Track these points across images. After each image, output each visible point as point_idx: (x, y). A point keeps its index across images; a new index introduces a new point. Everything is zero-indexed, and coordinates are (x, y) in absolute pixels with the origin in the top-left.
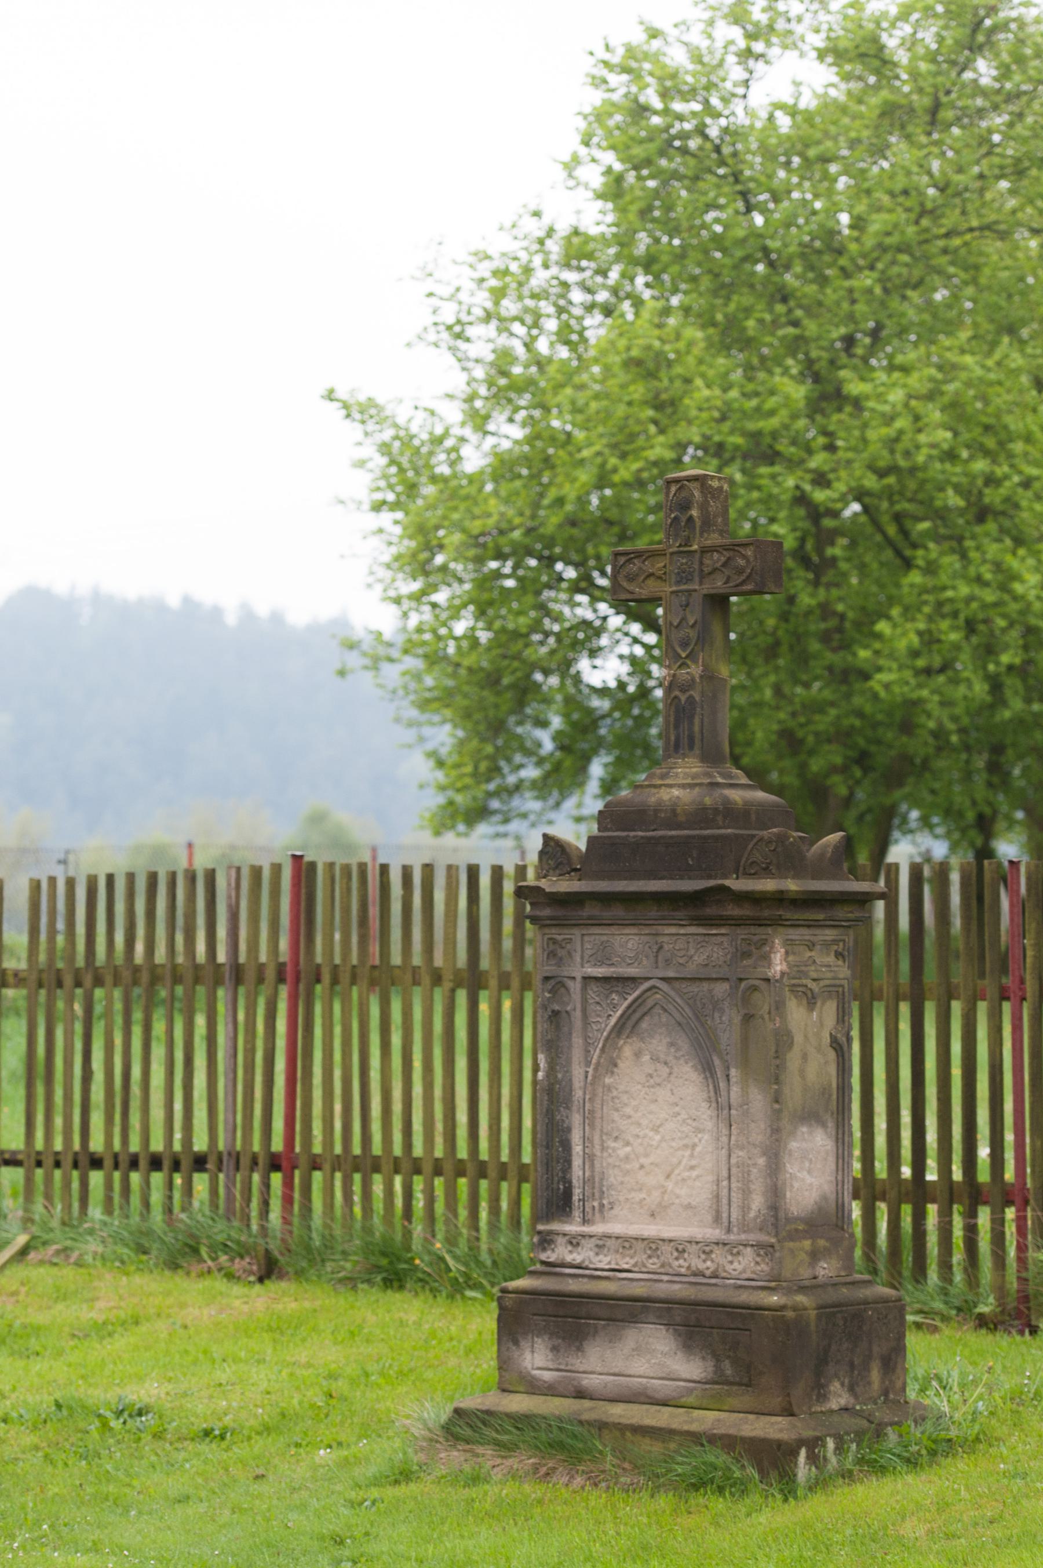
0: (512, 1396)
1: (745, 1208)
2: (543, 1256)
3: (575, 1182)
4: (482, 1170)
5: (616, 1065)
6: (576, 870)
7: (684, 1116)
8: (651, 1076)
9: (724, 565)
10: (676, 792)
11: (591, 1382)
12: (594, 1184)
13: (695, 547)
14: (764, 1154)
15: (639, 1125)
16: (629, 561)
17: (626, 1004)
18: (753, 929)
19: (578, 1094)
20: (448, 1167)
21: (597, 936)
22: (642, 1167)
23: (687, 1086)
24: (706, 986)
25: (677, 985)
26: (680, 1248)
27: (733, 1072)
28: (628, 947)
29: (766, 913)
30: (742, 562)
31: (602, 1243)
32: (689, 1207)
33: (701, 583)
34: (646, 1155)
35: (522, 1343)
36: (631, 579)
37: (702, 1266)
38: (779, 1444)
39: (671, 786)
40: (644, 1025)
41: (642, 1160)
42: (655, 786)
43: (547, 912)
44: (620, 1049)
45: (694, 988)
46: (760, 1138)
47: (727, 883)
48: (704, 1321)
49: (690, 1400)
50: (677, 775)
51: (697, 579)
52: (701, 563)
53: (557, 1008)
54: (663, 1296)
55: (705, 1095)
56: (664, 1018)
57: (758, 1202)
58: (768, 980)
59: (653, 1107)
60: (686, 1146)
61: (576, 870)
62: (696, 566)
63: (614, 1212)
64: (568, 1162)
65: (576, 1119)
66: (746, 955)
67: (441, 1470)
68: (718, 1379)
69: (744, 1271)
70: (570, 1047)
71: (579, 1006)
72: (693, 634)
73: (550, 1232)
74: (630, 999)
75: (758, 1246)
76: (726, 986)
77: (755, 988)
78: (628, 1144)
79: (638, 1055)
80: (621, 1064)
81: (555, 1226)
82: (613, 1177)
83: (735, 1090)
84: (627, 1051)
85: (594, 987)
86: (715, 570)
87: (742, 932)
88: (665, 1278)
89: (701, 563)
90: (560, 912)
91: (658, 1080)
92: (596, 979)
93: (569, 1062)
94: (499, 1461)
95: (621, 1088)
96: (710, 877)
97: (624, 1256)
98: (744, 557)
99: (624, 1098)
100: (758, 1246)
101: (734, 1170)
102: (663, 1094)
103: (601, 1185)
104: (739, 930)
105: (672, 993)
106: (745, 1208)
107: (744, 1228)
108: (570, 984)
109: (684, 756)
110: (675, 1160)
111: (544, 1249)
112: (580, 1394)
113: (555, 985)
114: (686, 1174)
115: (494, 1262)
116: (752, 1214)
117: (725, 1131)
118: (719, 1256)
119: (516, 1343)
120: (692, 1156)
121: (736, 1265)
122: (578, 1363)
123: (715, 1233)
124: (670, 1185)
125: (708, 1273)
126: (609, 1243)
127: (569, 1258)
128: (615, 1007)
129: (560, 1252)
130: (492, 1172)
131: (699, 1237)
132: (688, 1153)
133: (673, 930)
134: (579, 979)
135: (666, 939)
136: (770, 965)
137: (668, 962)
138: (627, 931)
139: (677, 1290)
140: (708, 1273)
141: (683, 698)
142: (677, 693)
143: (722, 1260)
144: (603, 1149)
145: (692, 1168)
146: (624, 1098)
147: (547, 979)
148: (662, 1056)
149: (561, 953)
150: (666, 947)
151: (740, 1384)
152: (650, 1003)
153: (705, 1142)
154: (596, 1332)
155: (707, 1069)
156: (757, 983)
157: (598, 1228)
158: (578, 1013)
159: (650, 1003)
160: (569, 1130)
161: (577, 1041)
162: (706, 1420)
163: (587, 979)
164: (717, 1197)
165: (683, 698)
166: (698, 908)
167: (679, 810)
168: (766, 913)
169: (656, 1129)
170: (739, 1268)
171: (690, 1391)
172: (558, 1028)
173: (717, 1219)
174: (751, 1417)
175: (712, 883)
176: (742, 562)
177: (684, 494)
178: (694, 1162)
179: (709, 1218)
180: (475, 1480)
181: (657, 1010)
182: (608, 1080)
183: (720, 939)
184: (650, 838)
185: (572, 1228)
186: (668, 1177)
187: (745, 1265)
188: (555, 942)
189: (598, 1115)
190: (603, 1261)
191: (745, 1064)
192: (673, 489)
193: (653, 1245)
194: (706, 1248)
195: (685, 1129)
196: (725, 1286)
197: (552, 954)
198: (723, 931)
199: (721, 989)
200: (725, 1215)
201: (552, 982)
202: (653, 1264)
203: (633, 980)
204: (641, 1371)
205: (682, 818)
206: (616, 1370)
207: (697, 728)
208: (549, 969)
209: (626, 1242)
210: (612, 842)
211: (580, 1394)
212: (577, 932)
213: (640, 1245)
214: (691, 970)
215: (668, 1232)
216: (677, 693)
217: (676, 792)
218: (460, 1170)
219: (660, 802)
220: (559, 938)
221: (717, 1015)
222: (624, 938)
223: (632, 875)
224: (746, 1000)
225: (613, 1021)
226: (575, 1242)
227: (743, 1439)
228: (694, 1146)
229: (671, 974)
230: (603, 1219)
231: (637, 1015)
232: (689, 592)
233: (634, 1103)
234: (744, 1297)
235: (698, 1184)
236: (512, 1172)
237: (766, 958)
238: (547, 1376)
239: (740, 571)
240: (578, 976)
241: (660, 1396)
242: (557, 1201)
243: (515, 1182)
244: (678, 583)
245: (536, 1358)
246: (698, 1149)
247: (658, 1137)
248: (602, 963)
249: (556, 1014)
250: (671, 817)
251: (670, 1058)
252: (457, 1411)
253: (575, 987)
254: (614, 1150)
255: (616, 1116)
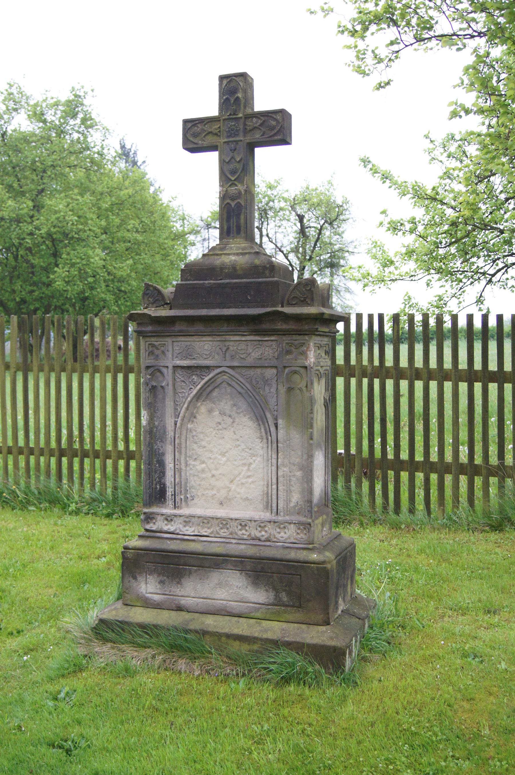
0: (134, 609)
1: (288, 501)
2: (148, 527)
3: (168, 484)
4: (31, 452)
5: (195, 417)
6: (167, 304)
7: (243, 446)
8: (220, 423)
9: (261, 125)
10: (233, 258)
11: (184, 602)
12: (182, 487)
13: (240, 115)
14: (301, 469)
15: (211, 452)
16: (194, 125)
17: (203, 382)
18: (294, 337)
19: (170, 434)
20: (14, 450)
21: (183, 342)
22: (213, 476)
23: (246, 429)
24: (259, 371)
25: (239, 370)
26: (243, 524)
27: (280, 422)
28: (205, 348)
29: (306, 327)
30: (274, 123)
31: (188, 520)
32: (247, 499)
33: (245, 136)
34: (217, 469)
35: (139, 578)
36: (195, 135)
37: (258, 535)
38: (335, 649)
39: (229, 254)
40: (215, 394)
41: (214, 472)
42: (217, 255)
43: (149, 328)
44: (198, 408)
45: (252, 372)
46: (297, 460)
47: (280, 309)
48: (261, 568)
49: (258, 615)
50: (231, 248)
51: (241, 134)
52: (245, 124)
53: (155, 384)
54: (237, 553)
55: (258, 435)
56: (229, 390)
57: (296, 498)
58: (306, 367)
59: (221, 441)
60: (244, 464)
61: (167, 304)
62: (241, 127)
63: (196, 501)
64: (163, 473)
65: (169, 448)
66: (289, 352)
67: (100, 662)
68: (278, 602)
69: (289, 538)
70: (164, 406)
71: (171, 383)
72: (240, 167)
73: (153, 513)
74: (207, 379)
75: (299, 524)
76: (274, 371)
77: (295, 372)
78: (203, 462)
79: (210, 411)
80: (198, 417)
81: (155, 509)
82: (193, 482)
83: (282, 433)
84: (203, 409)
85: (180, 371)
86: (255, 128)
87: (286, 339)
88: (234, 541)
89: (245, 124)
90: (159, 328)
91: (225, 426)
92: (182, 367)
93: (163, 415)
94: (136, 654)
95: (199, 430)
96: (263, 306)
97: (203, 528)
98: (275, 119)
99: (201, 436)
100: (299, 524)
101: (281, 479)
102: (228, 434)
103: (186, 486)
104: (284, 338)
105: (237, 376)
106: (288, 501)
107: (288, 512)
108: (164, 370)
109: (234, 238)
110: (236, 472)
111: (148, 523)
112: (179, 609)
113: (154, 371)
114: (244, 481)
115: (40, 493)
116: (292, 504)
117: (274, 456)
118: (269, 528)
119: (135, 578)
120: (248, 470)
121: (282, 534)
122: (177, 590)
123: (267, 516)
124: (233, 487)
125: (263, 539)
126: (193, 520)
127: (166, 528)
128: (195, 384)
129: (159, 524)
130: (36, 452)
131: (257, 518)
132: (246, 468)
133: (237, 338)
134: (171, 367)
135: (231, 343)
136: (306, 358)
137: (233, 357)
138: (205, 339)
139: (242, 549)
140: (263, 539)
141: (233, 204)
142: (228, 201)
143: (273, 532)
144: (187, 465)
145: (249, 477)
146: (201, 436)
147: (148, 367)
148: (227, 412)
149: (157, 352)
150: (231, 348)
151: (293, 606)
152: (219, 381)
153: (258, 463)
154: (190, 573)
155: (260, 419)
156: (297, 369)
157: (185, 511)
158: (171, 387)
159: (219, 381)
160: (163, 454)
161: (169, 404)
162: (274, 629)
163: (175, 367)
164: (267, 493)
165: (233, 204)
166: (254, 325)
167: (238, 268)
168: (306, 327)
169: (223, 454)
170: (286, 536)
171: (259, 609)
172: (155, 396)
173: (267, 507)
174: (304, 626)
175: (268, 310)
176: (274, 123)
177: (232, 84)
178: (249, 474)
179: (261, 506)
180: (128, 672)
181: (224, 385)
182: (190, 426)
183: (270, 343)
184: (220, 284)
185: (168, 510)
186: (232, 482)
187: (290, 534)
188: (153, 346)
189: (183, 445)
190: (190, 530)
191: (288, 416)
192: (225, 82)
193: (224, 522)
194: (262, 524)
195: (244, 454)
196: (277, 547)
197: (151, 353)
198: (273, 338)
199: (270, 373)
200: (274, 505)
201: (152, 369)
202: (224, 532)
203: (208, 368)
204: (223, 597)
205: (240, 272)
206: (205, 596)
207: (242, 221)
208: (150, 362)
209: (205, 520)
210: (194, 287)
211: (179, 609)
212: (169, 340)
213: (216, 522)
214: (249, 361)
215: (234, 514)
216: (228, 201)
217: (233, 258)
218: (21, 451)
219: (223, 264)
220: (156, 343)
221: (267, 388)
222: (202, 343)
223: (209, 306)
224: (288, 379)
225: (195, 392)
226: (169, 519)
227: (309, 645)
228: (250, 464)
229: (236, 364)
230: (187, 506)
231: (210, 388)
232: (237, 142)
233: (207, 439)
234: (292, 555)
235: (252, 486)
236: (46, 452)
237: (304, 354)
238: (156, 597)
239: (272, 128)
240: (170, 366)
241: (236, 611)
242: (158, 495)
243: (48, 457)
244: (228, 137)
245: (149, 587)
246: (253, 466)
247: (224, 459)
248: (186, 358)
249: (154, 388)
250: (233, 271)
251: (233, 413)
252: (102, 621)
253: (168, 373)
254: (194, 466)
255: (195, 446)
